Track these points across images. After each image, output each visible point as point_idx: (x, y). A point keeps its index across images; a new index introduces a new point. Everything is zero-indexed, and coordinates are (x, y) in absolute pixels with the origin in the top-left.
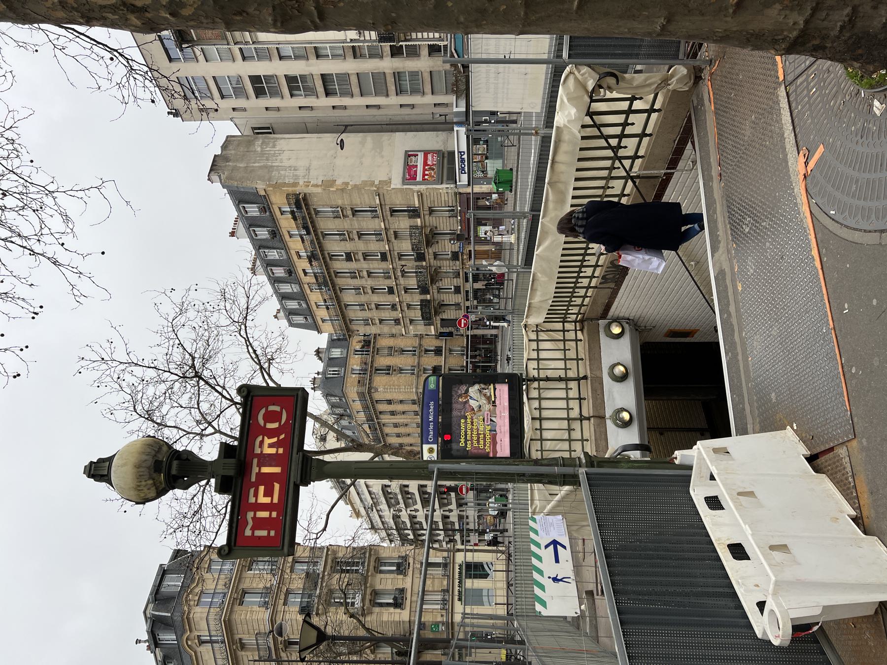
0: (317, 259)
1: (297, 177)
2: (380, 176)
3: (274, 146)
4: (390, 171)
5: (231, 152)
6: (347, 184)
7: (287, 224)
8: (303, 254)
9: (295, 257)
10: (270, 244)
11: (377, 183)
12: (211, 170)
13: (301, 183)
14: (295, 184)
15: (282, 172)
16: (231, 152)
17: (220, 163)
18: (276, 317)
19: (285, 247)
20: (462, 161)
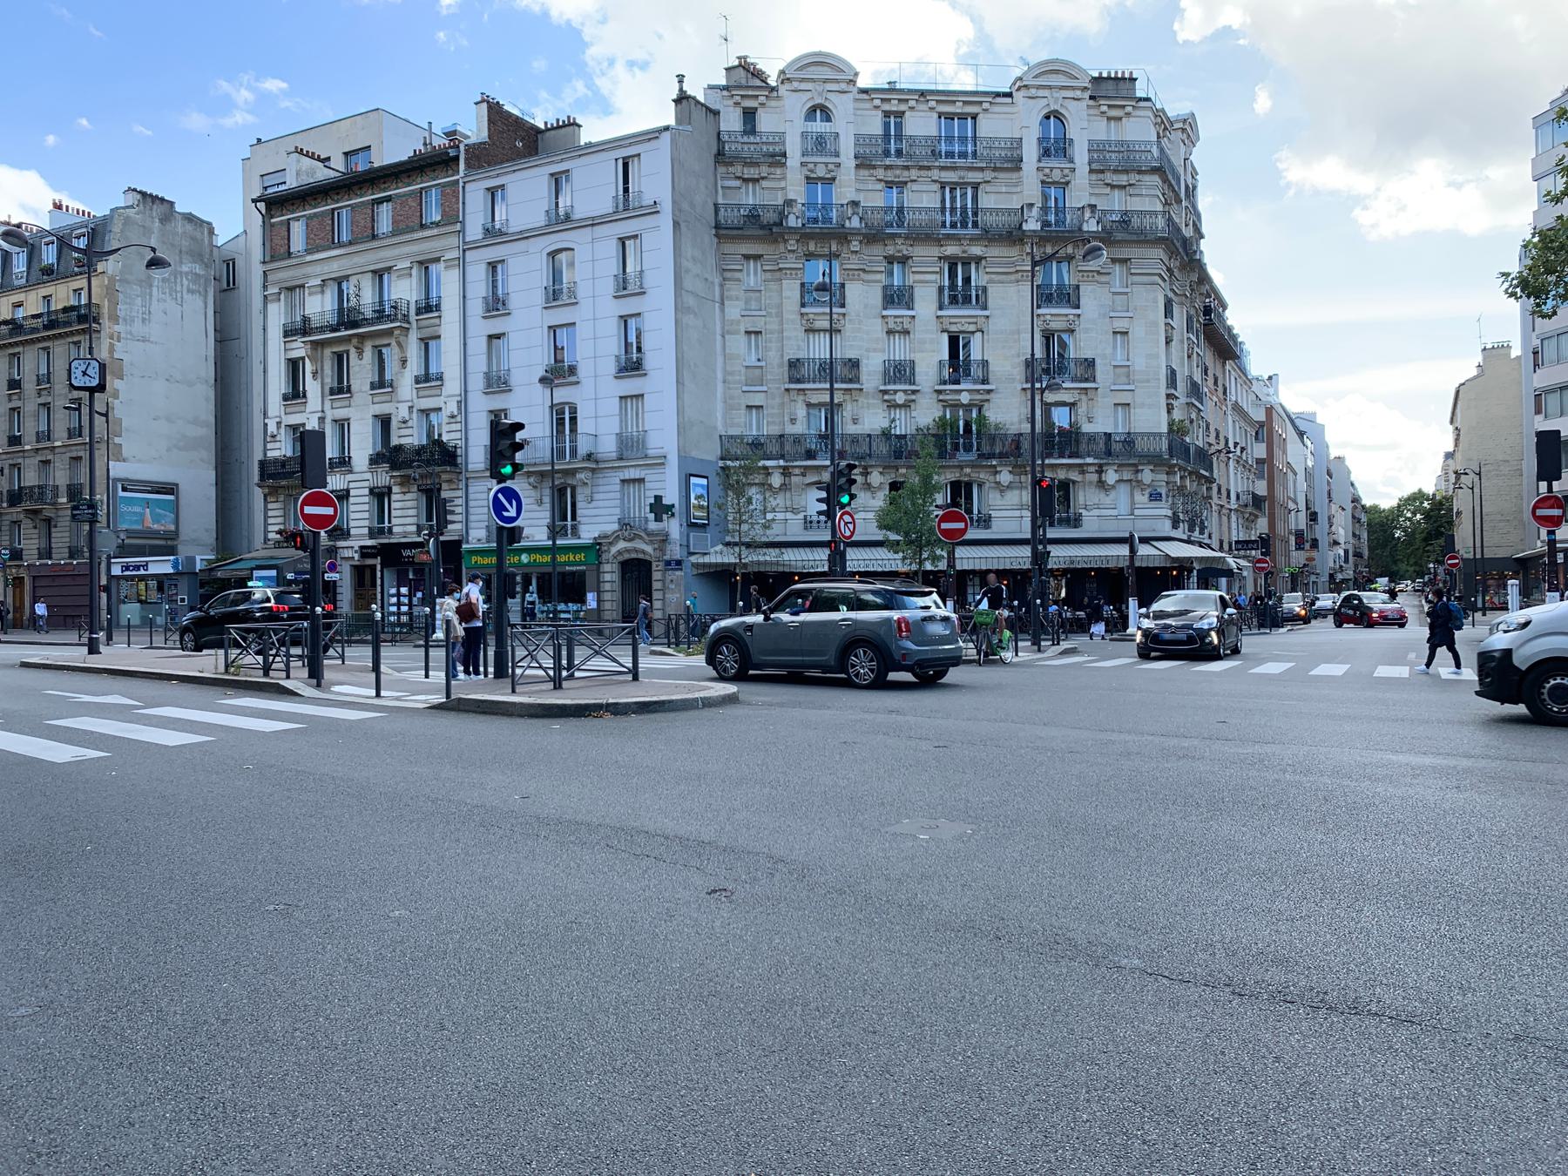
0: (11, 334)
1: (129, 321)
2: (127, 443)
3: (189, 291)
4: (140, 461)
5: (180, 227)
7: (62, 295)
8: (20, 313)
9: (16, 298)
10: (36, 266)
11: (117, 440)
12: (143, 194)
13: (116, 328)
14: (115, 319)
16: (180, 227)
17: (158, 210)
19: (30, 285)
20: (137, 568)
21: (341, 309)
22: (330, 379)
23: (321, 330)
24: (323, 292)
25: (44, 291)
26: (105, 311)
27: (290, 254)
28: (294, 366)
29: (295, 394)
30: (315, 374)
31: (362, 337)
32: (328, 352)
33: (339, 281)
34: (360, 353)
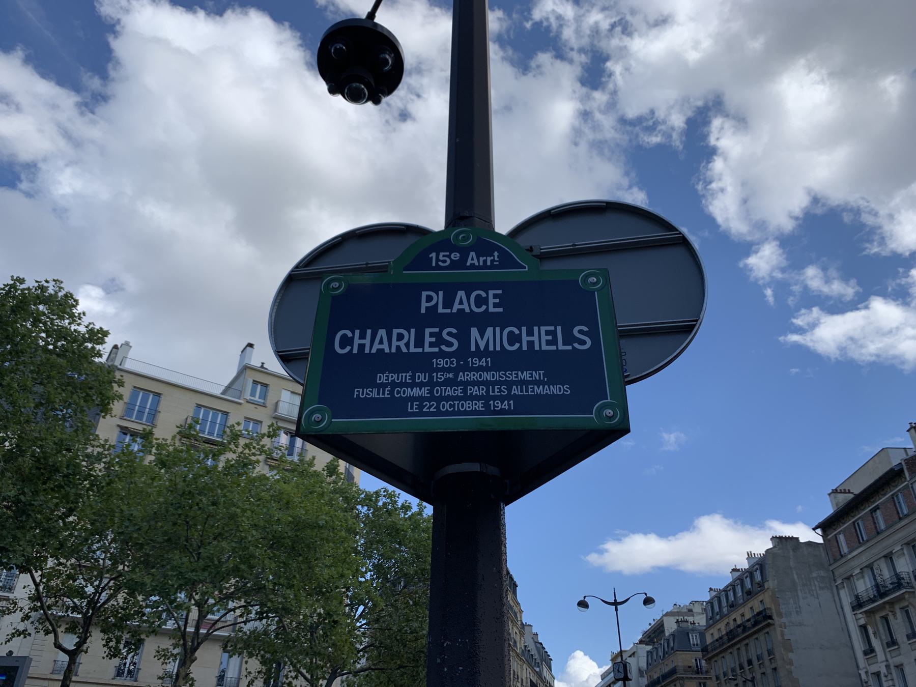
3: (821, 588)
6: (791, 663)
9: (741, 611)
13: (784, 620)
14: (780, 615)
15: (791, 601)
18: (711, 589)
21: (877, 586)
22: (886, 638)
23: (872, 601)
24: (863, 577)
25: (750, 605)
26: (774, 611)
27: (842, 556)
28: (864, 628)
29: (869, 651)
30: (875, 634)
31: (891, 603)
32: (878, 617)
33: (870, 567)
34: (895, 615)
